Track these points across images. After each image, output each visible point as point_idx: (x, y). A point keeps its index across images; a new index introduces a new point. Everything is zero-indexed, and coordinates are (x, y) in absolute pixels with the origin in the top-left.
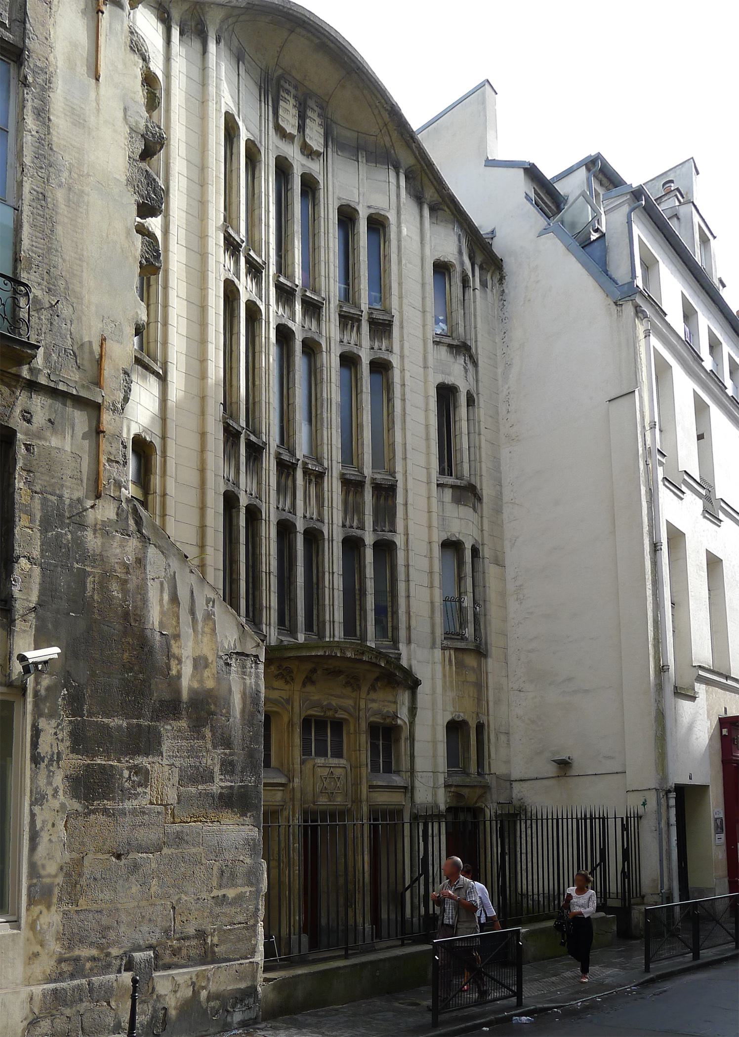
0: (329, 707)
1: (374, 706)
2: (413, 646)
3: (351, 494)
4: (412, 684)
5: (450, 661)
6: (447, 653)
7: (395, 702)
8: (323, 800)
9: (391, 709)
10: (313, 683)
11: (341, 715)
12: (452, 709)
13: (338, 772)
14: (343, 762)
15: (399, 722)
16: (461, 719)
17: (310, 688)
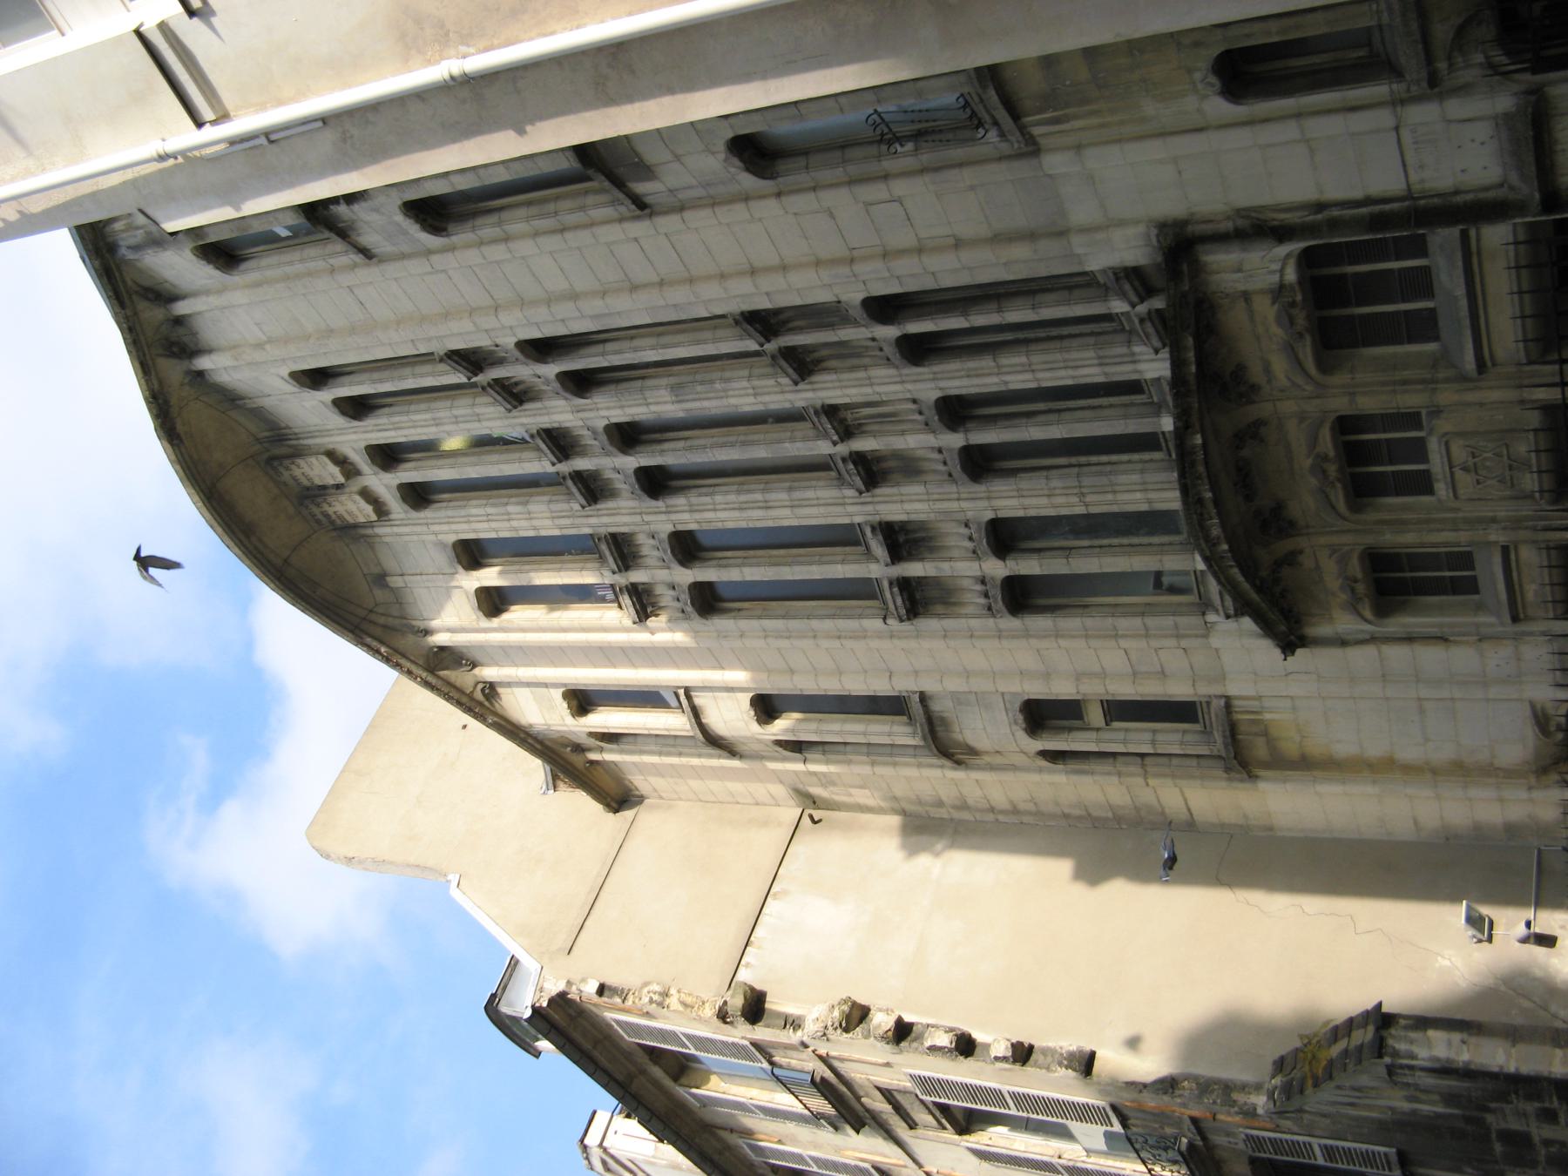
0: (1319, 469)
1: (1280, 365)
2: (1079, 250)
3: (816, 355)
4: (1181, 245)
5: (1056, 121)
6: (1036, 131)
7: (1246, 296)
8: (1530, 482)
9: (1266, 310)
10: (1279, 508)
11: (1326, 435)
12: (1190, 103)
13: (1459, 452)
14: (1434, 446)
15: (1291, 275)
16: (1213, 79)
17: (1294, 510)
